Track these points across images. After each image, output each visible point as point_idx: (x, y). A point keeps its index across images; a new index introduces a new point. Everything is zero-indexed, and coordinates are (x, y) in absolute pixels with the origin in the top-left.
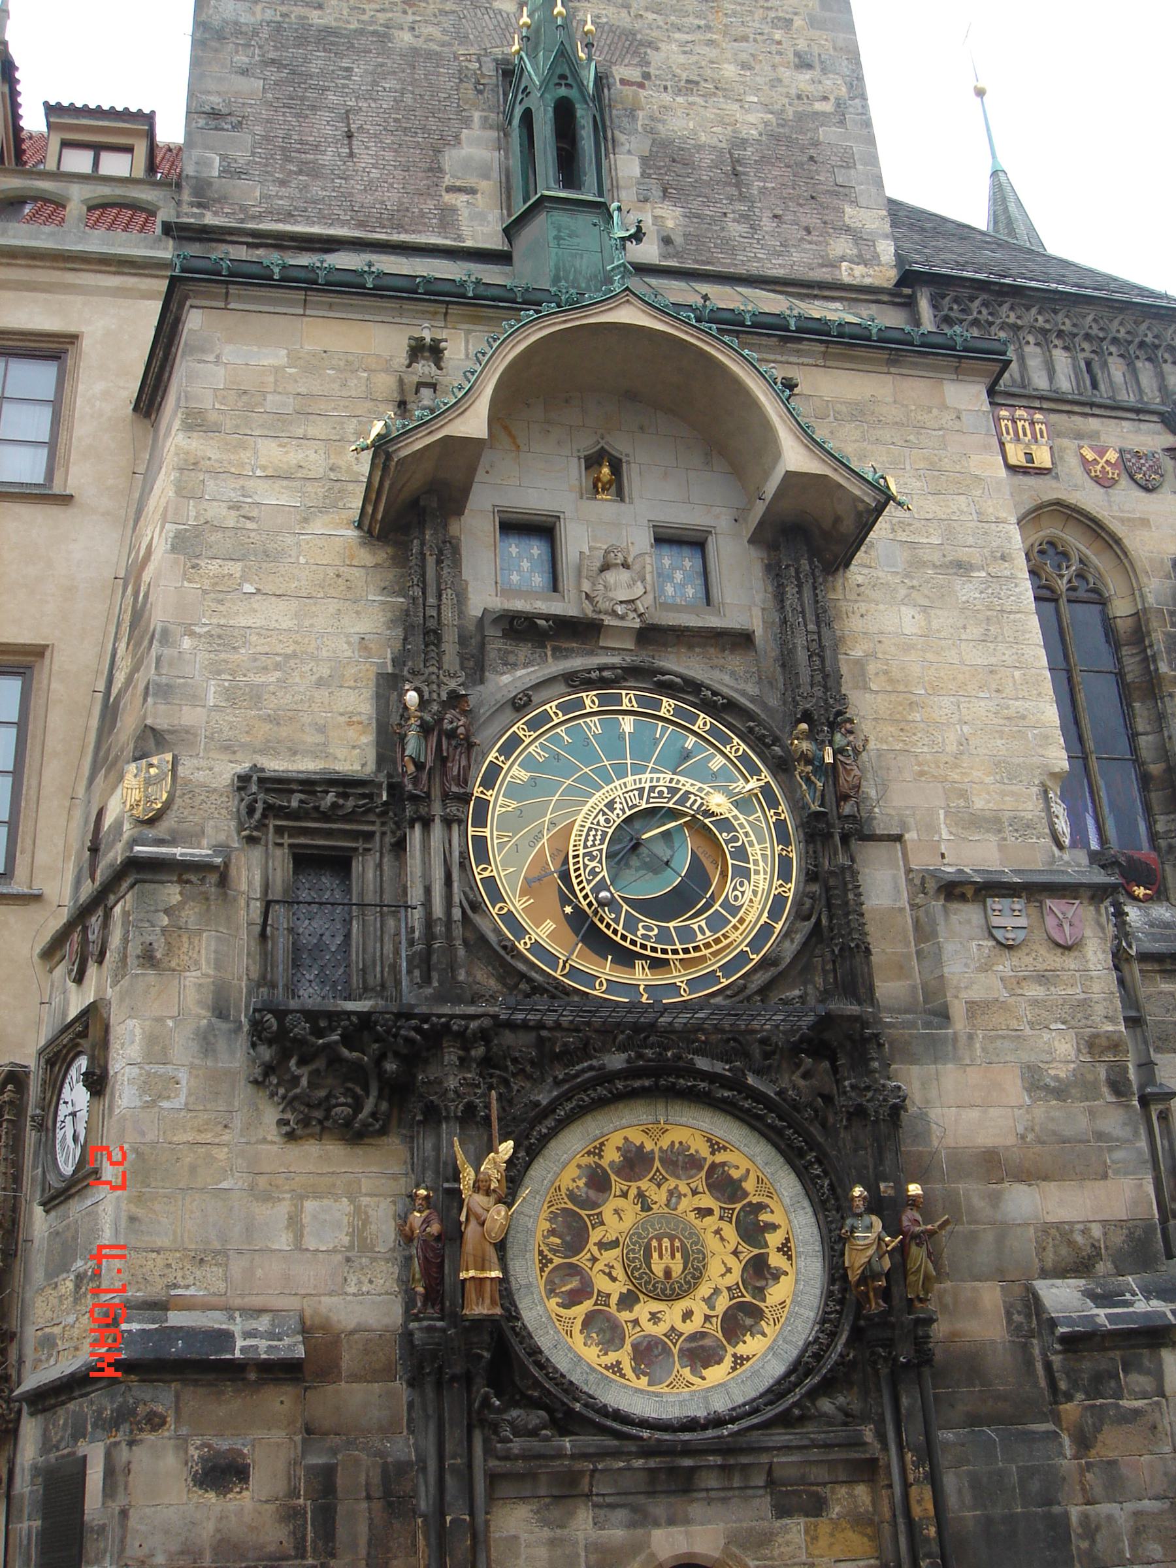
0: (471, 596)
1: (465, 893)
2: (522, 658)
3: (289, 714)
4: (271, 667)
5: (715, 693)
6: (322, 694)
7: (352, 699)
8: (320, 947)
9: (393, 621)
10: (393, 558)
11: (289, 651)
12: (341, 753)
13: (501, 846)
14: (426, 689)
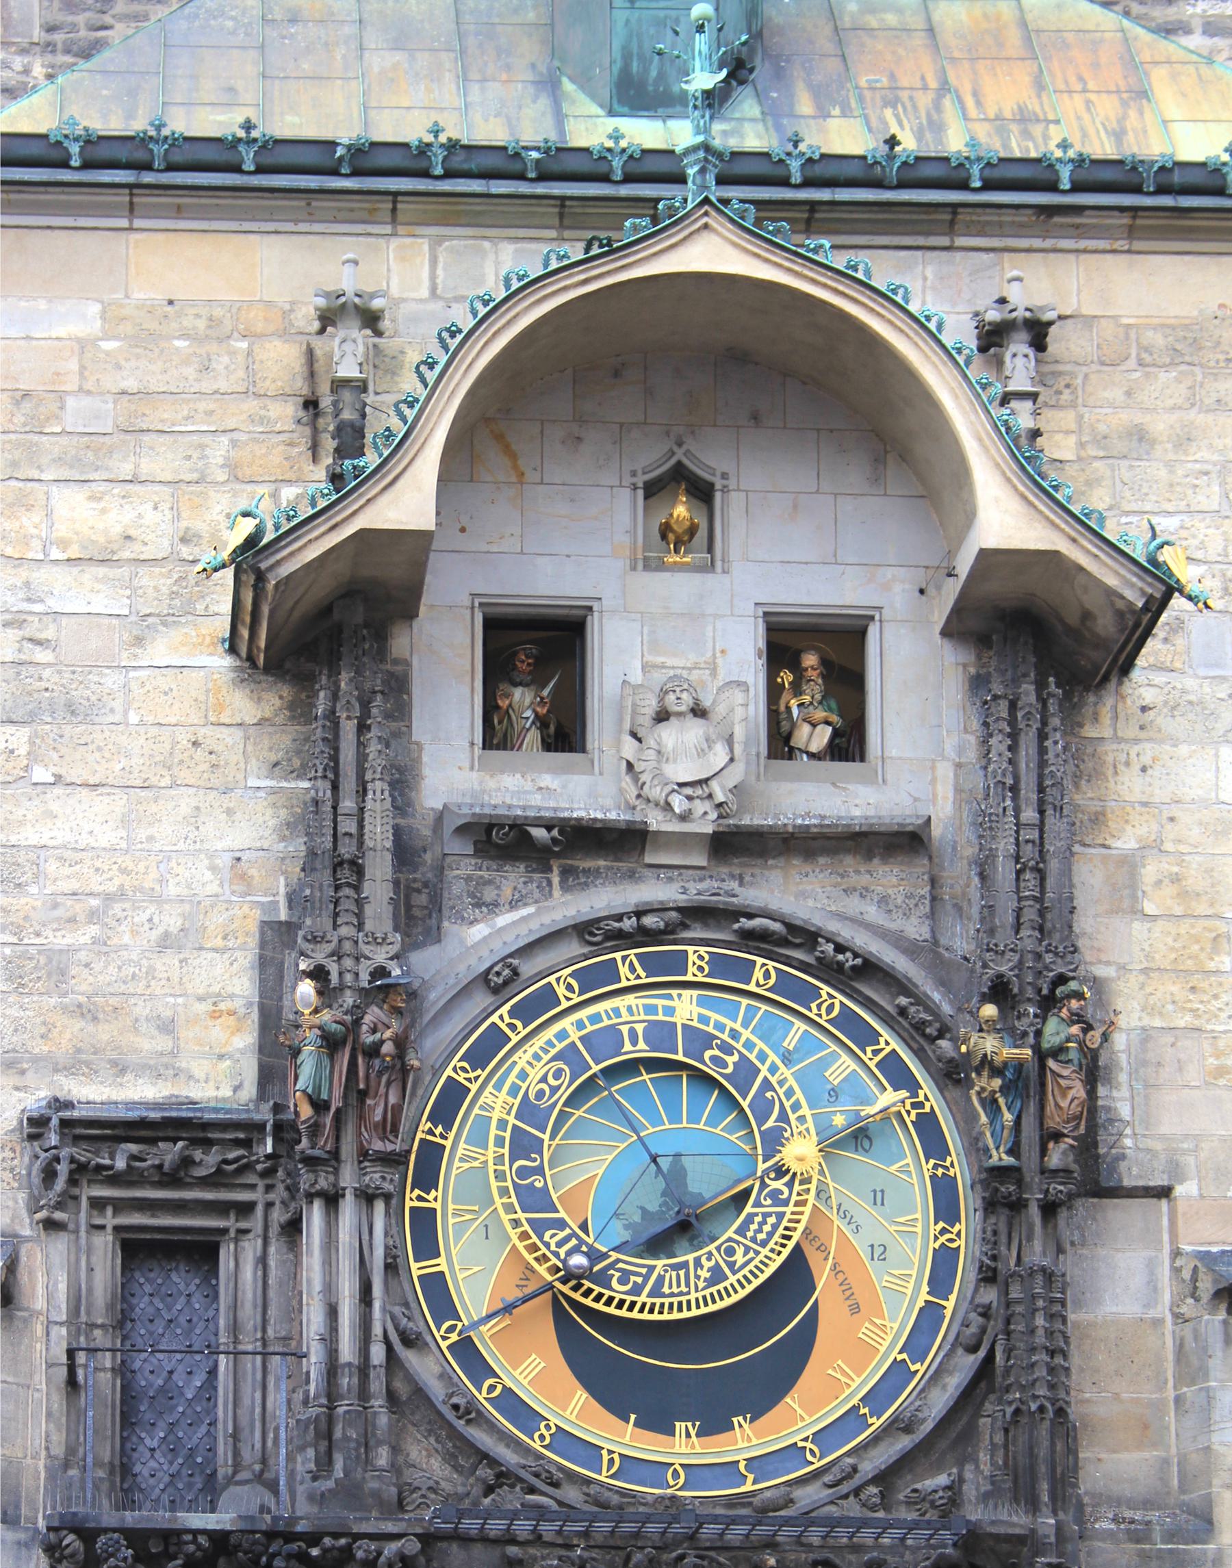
0: (426, 771)
1: (393, 1318)
2: (507, 892)
3: (113, 1001)
4: (81, 918)
5: (840, 948)
6: (168, 963)
7: (218, 970)
8: (168, 1393)
9: (289, 827)
10: (292, 706)
11: (112, 887)
12: (199, 1068)
13: (461, 1228)
14: (333, 969)
